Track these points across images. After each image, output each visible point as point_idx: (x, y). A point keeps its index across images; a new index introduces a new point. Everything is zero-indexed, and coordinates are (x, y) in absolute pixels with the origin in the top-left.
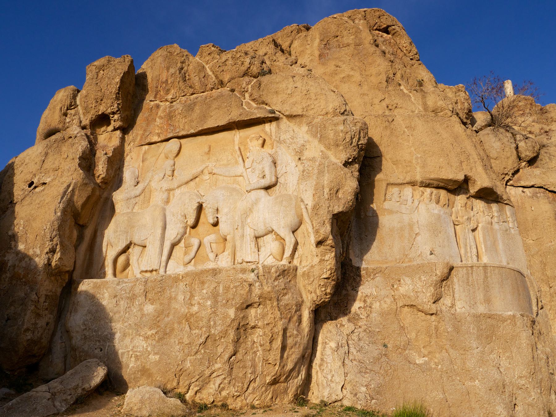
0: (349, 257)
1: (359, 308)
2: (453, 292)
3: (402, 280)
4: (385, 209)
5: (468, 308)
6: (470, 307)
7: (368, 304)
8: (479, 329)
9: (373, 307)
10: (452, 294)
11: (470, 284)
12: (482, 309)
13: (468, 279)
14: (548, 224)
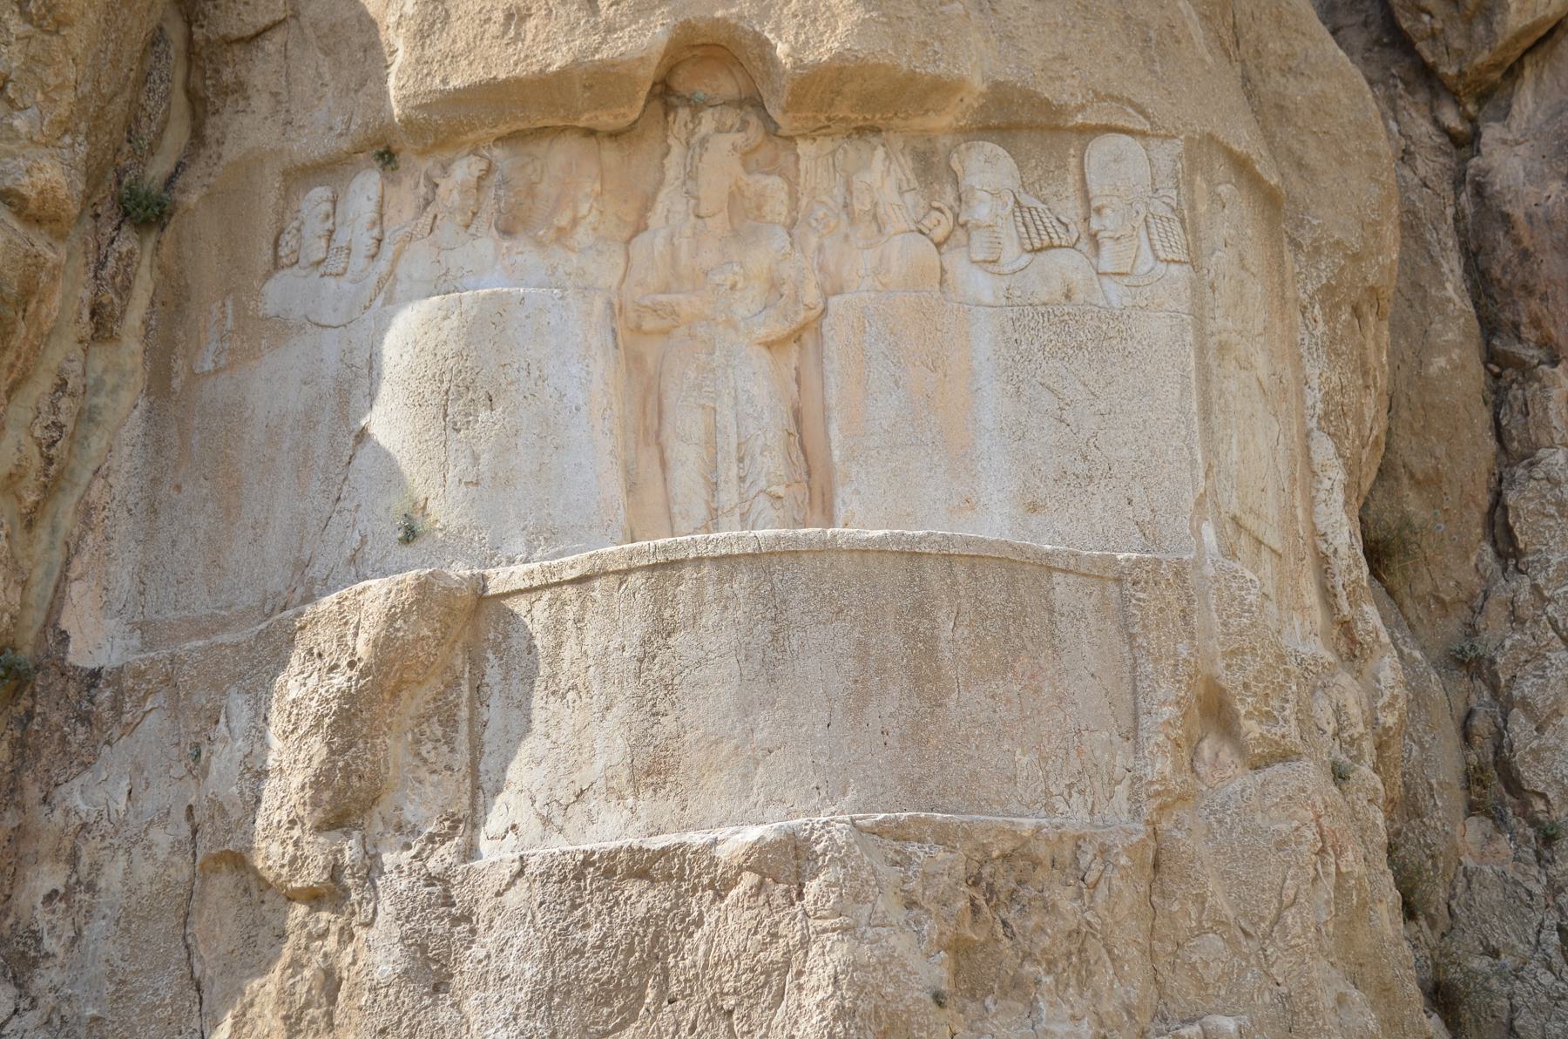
0: (55, 626)
1: (51, 897)
2: (476, 748)
3: (222, 719)
4: (266, 318)
5: (536, 827)
6: (546, 821)
7: (83, 869)
8: (562, 948)
9: (102, 884)
10: (462, 758)
12: (611, 830)
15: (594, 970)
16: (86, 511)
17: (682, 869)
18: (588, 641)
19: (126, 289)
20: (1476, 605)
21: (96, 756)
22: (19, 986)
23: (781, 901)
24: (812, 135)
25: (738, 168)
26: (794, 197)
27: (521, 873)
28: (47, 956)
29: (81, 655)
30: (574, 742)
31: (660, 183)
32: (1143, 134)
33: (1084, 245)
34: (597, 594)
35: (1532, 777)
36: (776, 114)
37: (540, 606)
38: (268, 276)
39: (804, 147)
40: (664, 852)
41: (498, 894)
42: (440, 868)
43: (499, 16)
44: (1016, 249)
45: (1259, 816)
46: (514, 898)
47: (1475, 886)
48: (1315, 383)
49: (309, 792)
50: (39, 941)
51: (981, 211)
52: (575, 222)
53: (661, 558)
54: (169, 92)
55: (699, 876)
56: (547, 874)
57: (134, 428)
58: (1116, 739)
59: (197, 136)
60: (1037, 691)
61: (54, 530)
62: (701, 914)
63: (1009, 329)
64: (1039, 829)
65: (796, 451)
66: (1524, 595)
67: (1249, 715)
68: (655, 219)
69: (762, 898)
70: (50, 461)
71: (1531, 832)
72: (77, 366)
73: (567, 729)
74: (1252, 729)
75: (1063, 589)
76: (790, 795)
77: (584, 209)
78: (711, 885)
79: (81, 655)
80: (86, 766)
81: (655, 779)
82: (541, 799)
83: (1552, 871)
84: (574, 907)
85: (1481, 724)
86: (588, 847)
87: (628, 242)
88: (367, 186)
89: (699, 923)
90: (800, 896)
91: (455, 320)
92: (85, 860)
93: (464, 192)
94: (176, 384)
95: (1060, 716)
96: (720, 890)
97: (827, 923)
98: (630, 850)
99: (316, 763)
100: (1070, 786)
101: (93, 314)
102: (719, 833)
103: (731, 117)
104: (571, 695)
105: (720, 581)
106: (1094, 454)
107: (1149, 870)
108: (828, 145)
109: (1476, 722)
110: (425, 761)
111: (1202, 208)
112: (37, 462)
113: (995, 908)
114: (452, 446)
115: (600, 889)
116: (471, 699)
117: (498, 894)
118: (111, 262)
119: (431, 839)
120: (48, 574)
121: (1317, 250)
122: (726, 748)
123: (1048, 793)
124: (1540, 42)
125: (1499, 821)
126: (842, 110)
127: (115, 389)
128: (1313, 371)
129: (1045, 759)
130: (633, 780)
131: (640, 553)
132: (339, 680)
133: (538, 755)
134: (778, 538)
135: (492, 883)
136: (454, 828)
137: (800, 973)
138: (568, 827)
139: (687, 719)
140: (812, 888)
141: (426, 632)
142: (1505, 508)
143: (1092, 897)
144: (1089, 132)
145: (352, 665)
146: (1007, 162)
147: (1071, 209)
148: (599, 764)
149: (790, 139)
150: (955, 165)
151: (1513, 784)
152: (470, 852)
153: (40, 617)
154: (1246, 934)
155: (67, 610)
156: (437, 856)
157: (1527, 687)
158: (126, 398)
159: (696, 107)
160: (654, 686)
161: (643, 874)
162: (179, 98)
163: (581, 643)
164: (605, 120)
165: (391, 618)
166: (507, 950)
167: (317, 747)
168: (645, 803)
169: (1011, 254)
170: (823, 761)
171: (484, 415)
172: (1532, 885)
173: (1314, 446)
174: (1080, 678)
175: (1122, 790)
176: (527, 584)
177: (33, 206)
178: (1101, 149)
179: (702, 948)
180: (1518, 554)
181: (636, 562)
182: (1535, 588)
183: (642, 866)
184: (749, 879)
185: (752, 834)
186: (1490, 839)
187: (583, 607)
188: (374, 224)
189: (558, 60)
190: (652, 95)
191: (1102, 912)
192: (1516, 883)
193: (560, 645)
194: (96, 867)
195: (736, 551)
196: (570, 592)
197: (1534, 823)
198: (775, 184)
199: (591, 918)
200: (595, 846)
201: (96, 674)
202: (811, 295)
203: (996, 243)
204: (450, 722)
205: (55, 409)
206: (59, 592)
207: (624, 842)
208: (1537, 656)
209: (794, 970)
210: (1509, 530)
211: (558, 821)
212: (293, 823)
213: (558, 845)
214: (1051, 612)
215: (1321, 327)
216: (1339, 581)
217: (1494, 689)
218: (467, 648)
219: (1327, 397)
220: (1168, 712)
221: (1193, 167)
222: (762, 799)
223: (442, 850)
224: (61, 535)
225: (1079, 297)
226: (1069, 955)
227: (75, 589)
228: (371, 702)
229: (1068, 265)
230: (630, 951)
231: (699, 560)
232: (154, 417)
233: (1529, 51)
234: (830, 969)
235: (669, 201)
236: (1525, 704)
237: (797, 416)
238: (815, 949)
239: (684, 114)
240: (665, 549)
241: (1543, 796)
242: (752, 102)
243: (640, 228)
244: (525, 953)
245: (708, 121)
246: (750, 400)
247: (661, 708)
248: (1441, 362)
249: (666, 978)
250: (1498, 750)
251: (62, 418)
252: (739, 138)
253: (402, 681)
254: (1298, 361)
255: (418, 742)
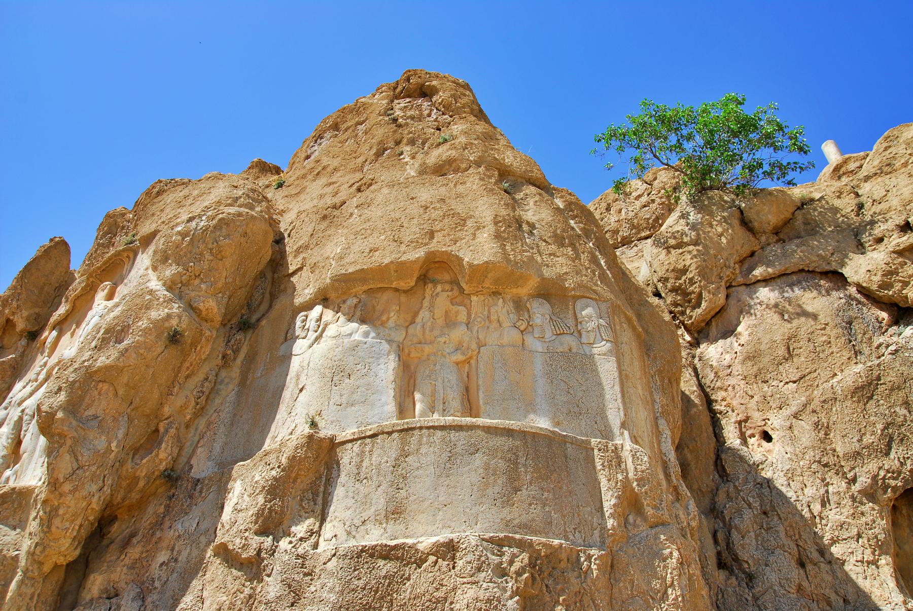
1: (162, 565)
5: (344, 536)
6: (349, 533)
7: (175, 553)
8: (346, 587)
9: (180, 559)
11: (362, 476)
12: (374, 537)
13: (359, 466)
14: (824, 338)
15: (361, 599)
16: (209, 424)
17: (403, 554)
18: (374, 459)
19: (236, 352)
20: (715, 492)
21: (190, 510)
22: (143, 601)
23: (445, 569)
24: (476, 293)
25: (449, 303)
26: (469, 315)
27: (334, 555)
28: (155, 588)
29: (195, 473)
30: (364, 500)
31: (421, 308)
32: (596, 300)
33: (576, 334)
34: (379, 441)
35: (743, 555)
36: (464, 285)
37: (356, 446)
38: (282, 343)
39: (474, 298)
40: (396, 547)
41: (325, 564)
42: (303, 552)
43: (367, 250)
44: (551, 334)
45: (654, 547)
46: (330, 565)
47: (725, 596)
48: (658, 401)
49: (254, 518)
50: (154, 582)
51: (537, 320)
52: (388, 319)
53: (406, 427)
54: (263, 294)
55: (410, 558)
56: (345, 555)
57: (232, 397)
58: (594, 511)
59: (270, 306)
60: (561, 488)
61: (196, 429)
62: (410, 575)
63: (548, 360)
64: (561, 544)
65: (466, 401)
66: (731, 489)
67: (648, 505)
68: (418, 320)
69: (437, 567)
70: (197, 404)
71: (743, 576)
72: (214, 373)
73: (361, 495)
74: (649, 511)
75: (570, 449)
76: (453, 524)
77: (392, 314)
78: (415, 562)
79: (195, 473)
80: (186, 513)
81: (396, 516)
82: (348, 524)
83: (753, 591)
84: (355, 570)
85: (720, 536)
86: (364, 544)
87: (407, 327)
88: (318, 309)
89: (408, 579)
90: (454, 568)
91: (340, 349)
92: (177, 548)
93: (350, 308)
94: (248, 382)
95: (570, 499)
96: (420, 563)
97: (465, 580)
98: (381, 545)
99: (259, 506)
100: (575, 529)
101: (224, 357)
102: (420, 539)
103: (447, 287)
104: (365, 481)
105: (429, 435)
106: (581, 405)
107: (609, 568)
108: (482, 298)
109: (719, 534)
110: (304, 508)
111: (618, 328)
112: (193, 403)
113: (543, 580)
114: (333, 392)
115: (367, 562)
116: (325, 484)
117: (325, 564)
118: (232, 342)
119: (301, 539)
120: (191, 445)
121: (655, 358)
122: (427, 504)
123: (566, 531)
124: (717, 313)
125: (731, 572)
126: (487, 284)
127: (228, 384)
128: (657, 397)
129: (564, 517)
130: (386, 517)
131: (398, 425)
132: (274, 473)
133: (349, 505)
134: (454, 421)
135: (322, 559)
136: (311, 536)
137: (452, 603)
138: (357, 536)
139: (410, 491)
140: (460, 563)
141: (310, 455)
142: (721, 460)
143: (585, 577)
144: (576, 298)
145: (279, 467)
146: (547, 306)
147: (571, 322)
148: (373, 510)
149: (469, 295)
150: (528, 305)
151: (736, 559)
152: (316, 546)
153: (185, 460)
154: (653, 598)
155: (194, 457)
156: (302, 547)
157: (736, 521)
158: (231, 387)
159: (435, 282)
160: (400, 476)
161: (385, 558)
162: (267, 295)
163: (370, 460)
164: (403, 285)
165: (297, 448)
166: (325, 590)
167: (261, 499)
168: (391, 527)
169: (548, 335)
170: (468, 510)
171: (347, 381)
172: (746, 596)
173: (659, 422)
174: (578, 485)
175: (597, 533)
176: (352, 437)
177: (204, 313)
178: (579, 304)
179: (409, 590)
180: (727, 475)
181: (395, 428)
182: (735, 486)
183: (386, 553)
184: (432, 558)
185: (434, 539)
186: (729, 579)
187: (373, 446)
188: (317, 321)
189: (386, 261)
190: (419, 279)
191: (590, 584)
192: (741, 596)
193: (362, 461)
194: (179, 552)
195: (436, 424)
196: (368, 440)
197: (744, 572)
198: (461, 308)
199: (361, 575)
200: (367, 543)
201: (198, 480)
202: (474, 346)
203: (543, 331)
204: (315, 494)
205: (202, 386)
206: (194, 451)
207: (379, 542)
208: (739, 511)
209: (448, 602)
210: (723, 467)
211: (354, 533)
212: (246, 530)
213: (352, 543)
214: (566, 458)
215: (659, 383)
216: (672, 470)
217: (724, 522)
218: (326, 464)
219: (662, 406)
220: (613, 501)
221: (614, 313)
222: (440, 526)
223: (305, 545)
224: (199, 432)
225: (574, 350)
226: (575, 603)
227: (199, 450)
228: (284, 482)
229: (570, 341)
230: (376, 592)
231: (421, 428)
232: (239, 394)
233: (713, 317)
234: (465, 601)
235: (424, 315)
236: (737, 528)
237: (467, 389)
238: (459, 591)
239: (430, 285)
240: (407, 423)
241: (747, 562)
242: (455, 282)
243: (413, 322)
244: (331, 590)
245: (439, 288)
246: (449, 381)
247: (400, 486)
248: (695, 410)
249: (392, 605)
250: (728, 544)
251: (204, 389)
252: (450, 293)
253: (298, 474)
254: (651, 394)
255: (302, 500)
